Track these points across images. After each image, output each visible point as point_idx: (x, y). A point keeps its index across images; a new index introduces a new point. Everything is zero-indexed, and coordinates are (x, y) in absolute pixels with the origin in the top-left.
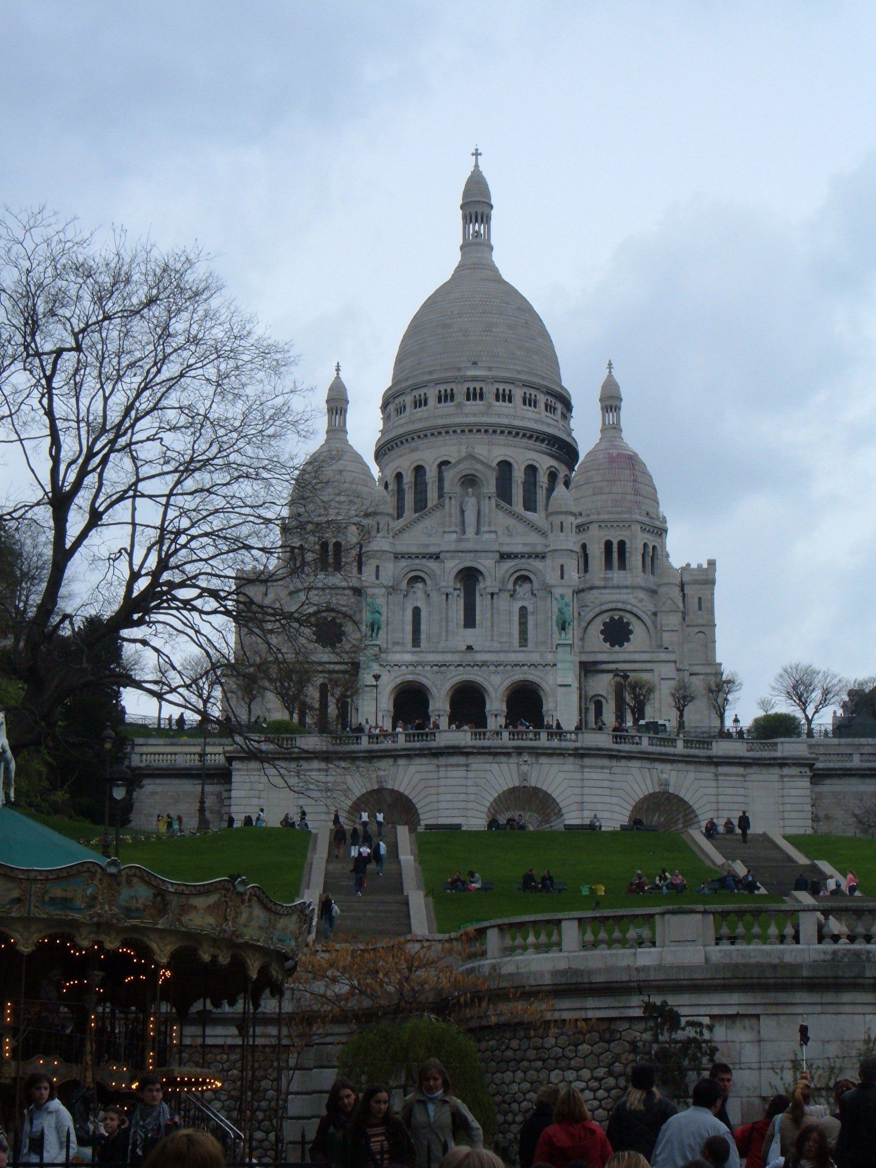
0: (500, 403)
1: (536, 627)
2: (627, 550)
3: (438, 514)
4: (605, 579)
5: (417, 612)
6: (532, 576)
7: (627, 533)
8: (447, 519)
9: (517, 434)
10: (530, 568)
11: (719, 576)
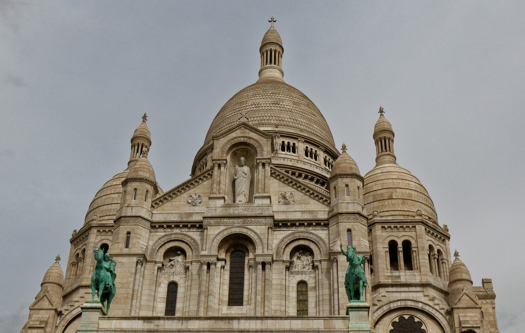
0: (286, 152)
1: (318, 304)
2: (413, 249)
3: (204, 183)
4: (391, 277)
5: (173, 287)
6: (313, 246)
7: (413, 234)
8: (215, 185)
9: (300, 175)
10: (310, 236)
11: (496, 290)
